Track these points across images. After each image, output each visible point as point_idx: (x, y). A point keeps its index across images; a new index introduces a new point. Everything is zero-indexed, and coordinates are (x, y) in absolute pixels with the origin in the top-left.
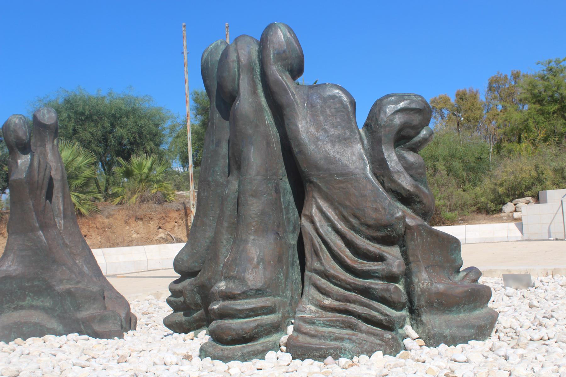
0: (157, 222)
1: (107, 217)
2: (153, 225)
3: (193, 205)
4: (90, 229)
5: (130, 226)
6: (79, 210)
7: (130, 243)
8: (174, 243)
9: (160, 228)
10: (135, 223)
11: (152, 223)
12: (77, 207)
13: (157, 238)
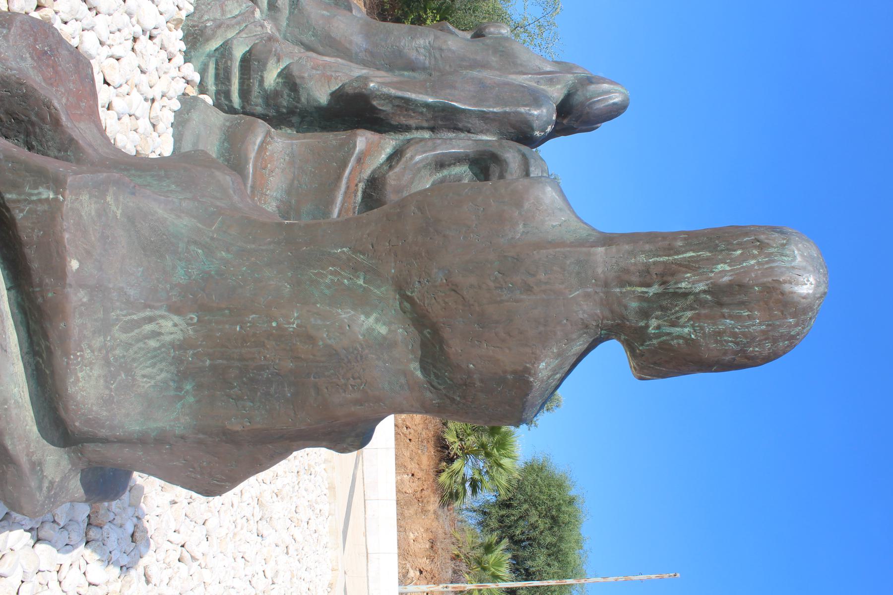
0: (428, 569)
1: (435, 512)
2: (424, 563)
3: (446, 587)
4: (421, 482)
5: (424, 532)
6: (444, 471)
7: (401, 528)
8: (396, 470)
9: (421, 572)
10: (427, 539)
11: (427, 562)
12: (447, 470)
13: (408, 565)
